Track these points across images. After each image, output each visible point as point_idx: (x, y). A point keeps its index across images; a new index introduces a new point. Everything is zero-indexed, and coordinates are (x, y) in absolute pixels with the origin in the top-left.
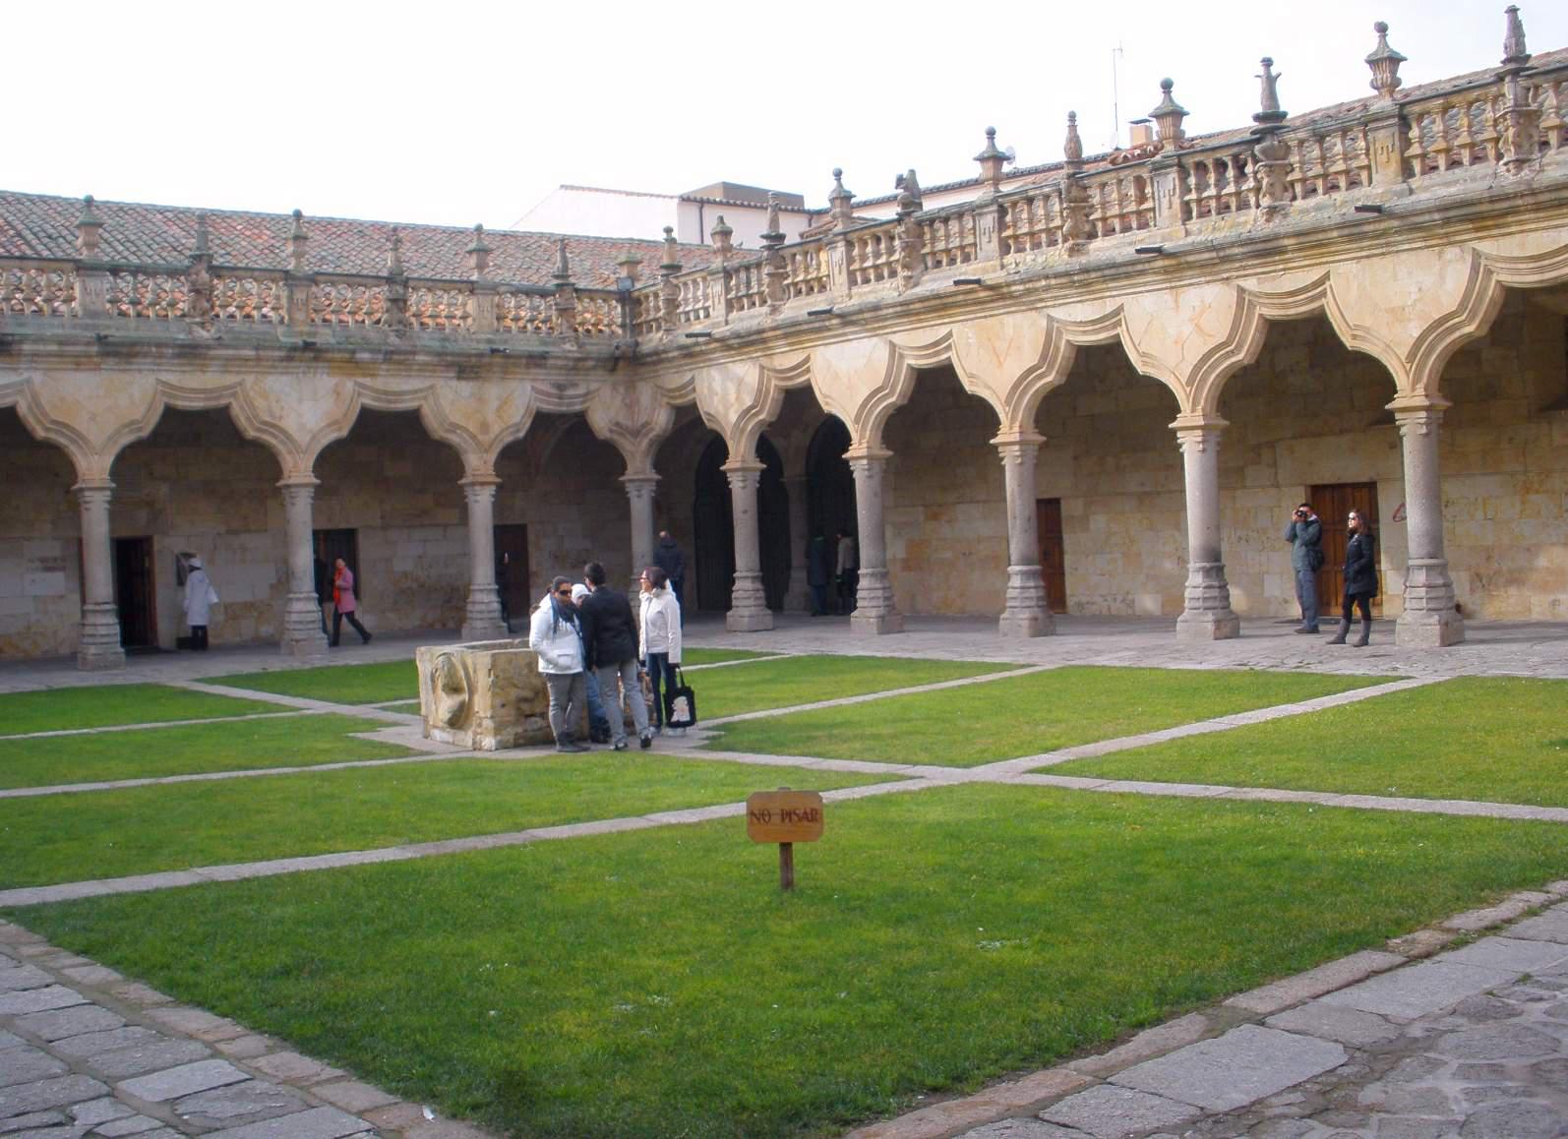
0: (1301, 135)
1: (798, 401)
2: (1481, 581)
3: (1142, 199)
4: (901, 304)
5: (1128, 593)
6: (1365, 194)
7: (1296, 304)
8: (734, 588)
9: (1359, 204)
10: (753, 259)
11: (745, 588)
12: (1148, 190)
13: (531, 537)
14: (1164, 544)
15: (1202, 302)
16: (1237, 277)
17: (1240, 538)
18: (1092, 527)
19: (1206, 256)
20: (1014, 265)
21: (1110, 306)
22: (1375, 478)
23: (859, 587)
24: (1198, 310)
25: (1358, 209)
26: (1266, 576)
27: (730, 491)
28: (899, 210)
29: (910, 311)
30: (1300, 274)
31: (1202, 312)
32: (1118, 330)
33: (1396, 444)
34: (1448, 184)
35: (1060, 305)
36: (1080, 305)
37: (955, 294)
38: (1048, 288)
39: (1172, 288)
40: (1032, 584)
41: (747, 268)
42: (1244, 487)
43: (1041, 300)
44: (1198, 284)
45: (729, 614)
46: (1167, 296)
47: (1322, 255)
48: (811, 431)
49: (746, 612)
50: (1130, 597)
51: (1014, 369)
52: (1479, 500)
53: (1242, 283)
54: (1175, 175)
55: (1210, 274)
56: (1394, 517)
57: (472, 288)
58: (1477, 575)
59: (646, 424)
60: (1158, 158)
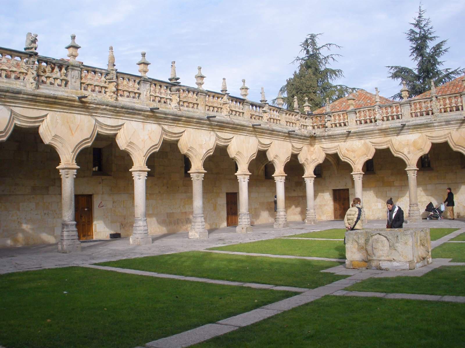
15: (152, 129)
16: (164, 124)
17: (45, 214)
19: (162, 115)
21: (120, 122)
26: (55, 228)
35: (102, 117)
36: (109, 119)
38: (105, 109)
39: (143, 122)
42: (48, 194)
43: (96, 113)
44: (151, 123)
46: (141, 124)
47: (187, 125)
55: (157, 121)
56: (99, 206)
58: (122, 224)
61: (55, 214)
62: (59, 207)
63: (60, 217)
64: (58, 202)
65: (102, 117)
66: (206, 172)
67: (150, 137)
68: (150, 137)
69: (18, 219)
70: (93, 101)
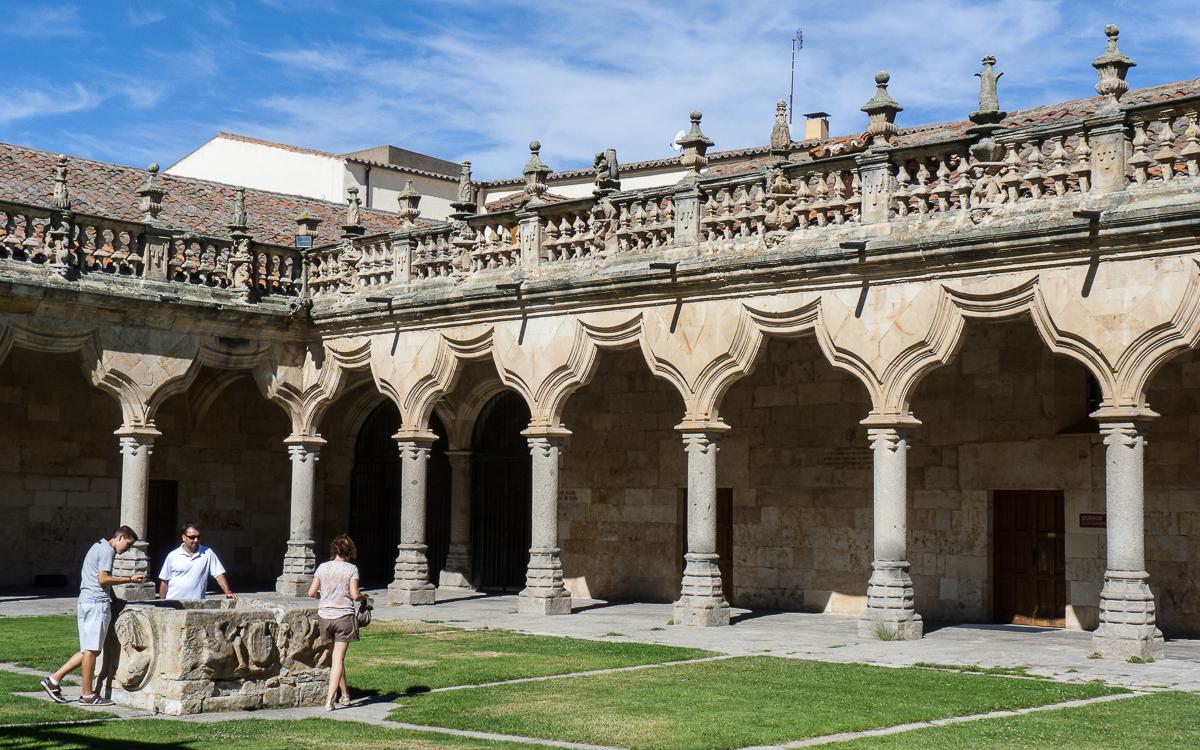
0: (1020, 136)
1: (476, 370)
2: (1172, 597)
3: (848, 193)
4: (593, 284)
5: (797, 587)
6: (1084, 200)
7: (999, 308)
8: (397, 560)
9: (1078, 210)
10: (441, 228)
11: (409, 560)
12: (855, 184)
13: (182, 494)
14: (838, 540)
15: (903, 299)
17: (916, 540)
18: (763, 518)
20: (711, 253)
21: (806, 298)
22: (1063, 487)
23: (528, 566)
24: (897, 307)
25: (1076, 214)
26: (942, 579)
27: (531, 457)
28: (597, 188)
29: (602, 295)
30: (1007, 277)
31: (900, 313)
32: (814, 324)
33: (1097, 454)
34: (1169, 193)
37: (650, 277)
40: (709, 573)
41: (434, 236)
42: (923, 487)
45: (389, 586)
48: (480, 405)
49: (408, 585)
50: (800, 592)
51: (704, 355)
52: (1174, 516)
53: (946, 282)
54: (886, 172)
57: (143, 236)
58: (1169, 591)
59: (316, 386)
60: (868, 152)
61: (943, 542)
62: (954, 523)
63: (956, 550)
64: (951, 510)
65: (755, 295)
66: (1156, 414)
67: (896, 324)
68: (896, 324)
69: (850, 547)
70: (713, 265)
